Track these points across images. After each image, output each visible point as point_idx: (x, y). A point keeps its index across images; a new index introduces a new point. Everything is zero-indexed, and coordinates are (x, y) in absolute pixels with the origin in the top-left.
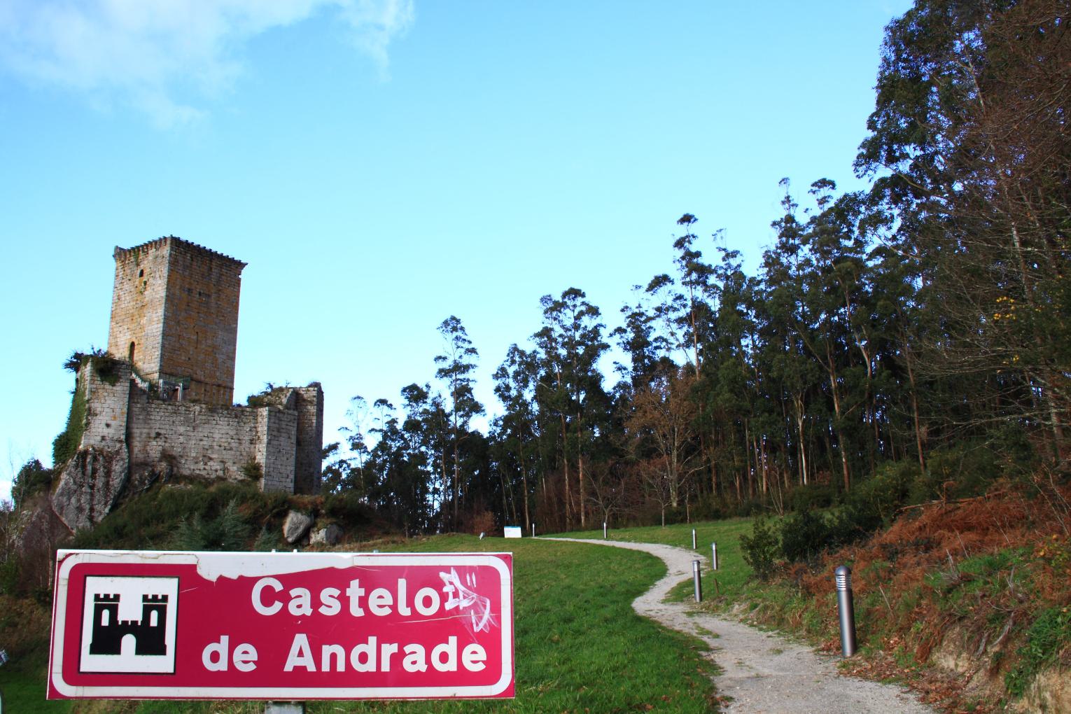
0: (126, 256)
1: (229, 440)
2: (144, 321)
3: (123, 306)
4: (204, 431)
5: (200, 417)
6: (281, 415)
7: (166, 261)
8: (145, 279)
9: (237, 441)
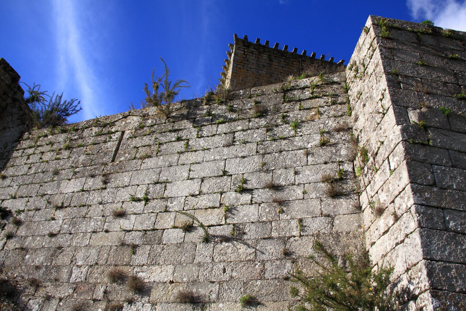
1: (231, 197)
4: (135, 180)
5: (137, 142)
9: (267, 194)
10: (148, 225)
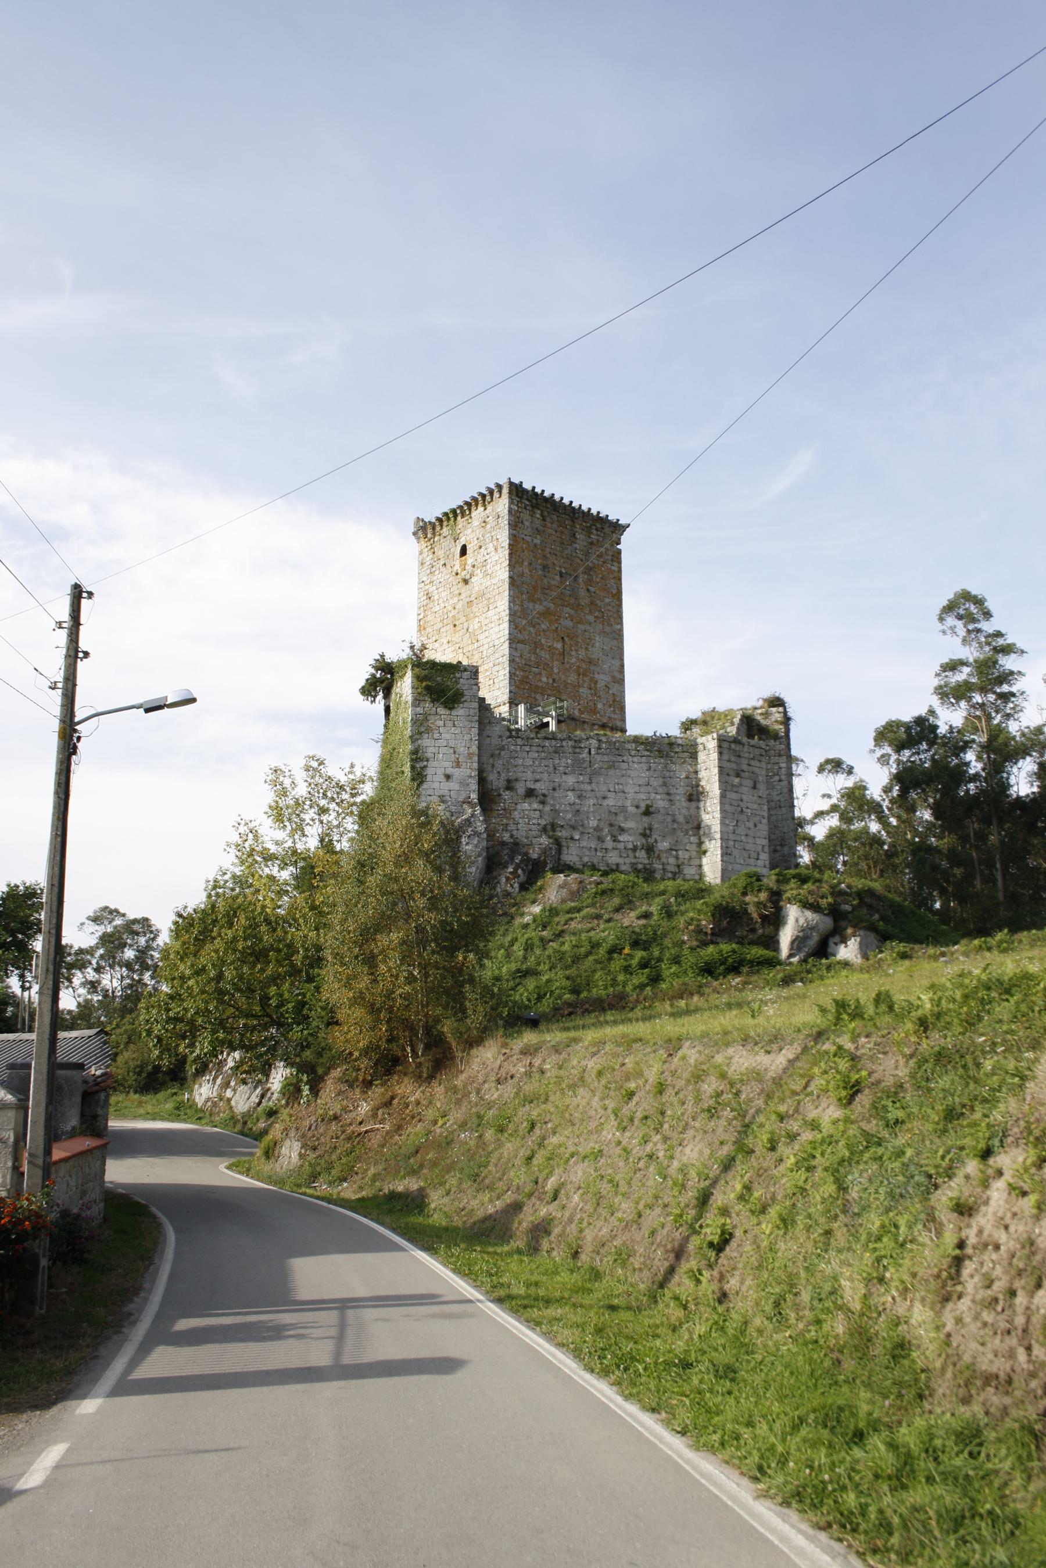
0: (434, 529)
2: (474, 625)
3: (437, 608)
6: (738, 748)
7: (505, 522)
8: (470, 559)
10: (620, 804)
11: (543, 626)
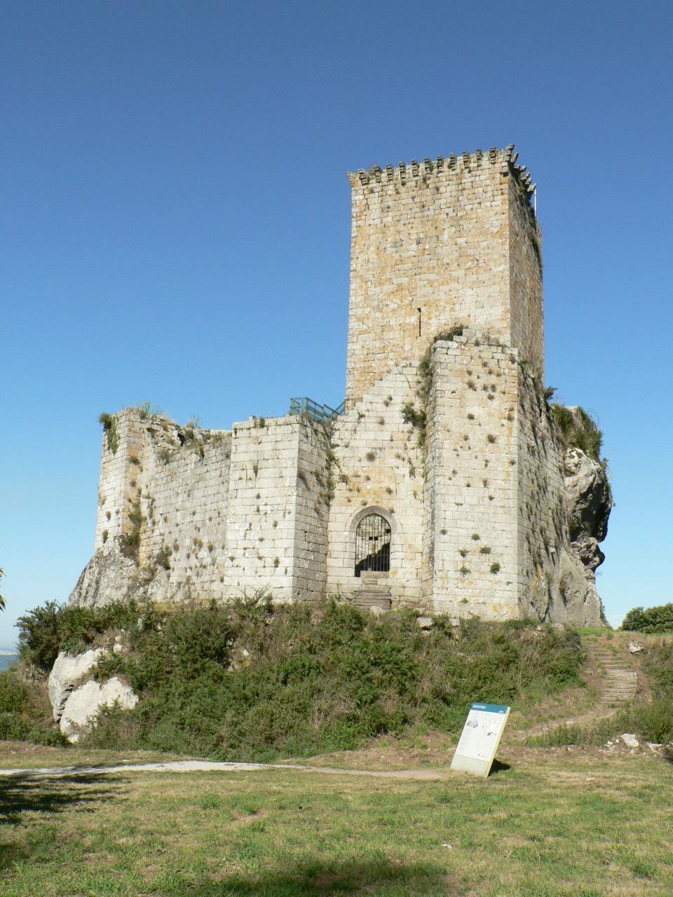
11: (392, 306)
